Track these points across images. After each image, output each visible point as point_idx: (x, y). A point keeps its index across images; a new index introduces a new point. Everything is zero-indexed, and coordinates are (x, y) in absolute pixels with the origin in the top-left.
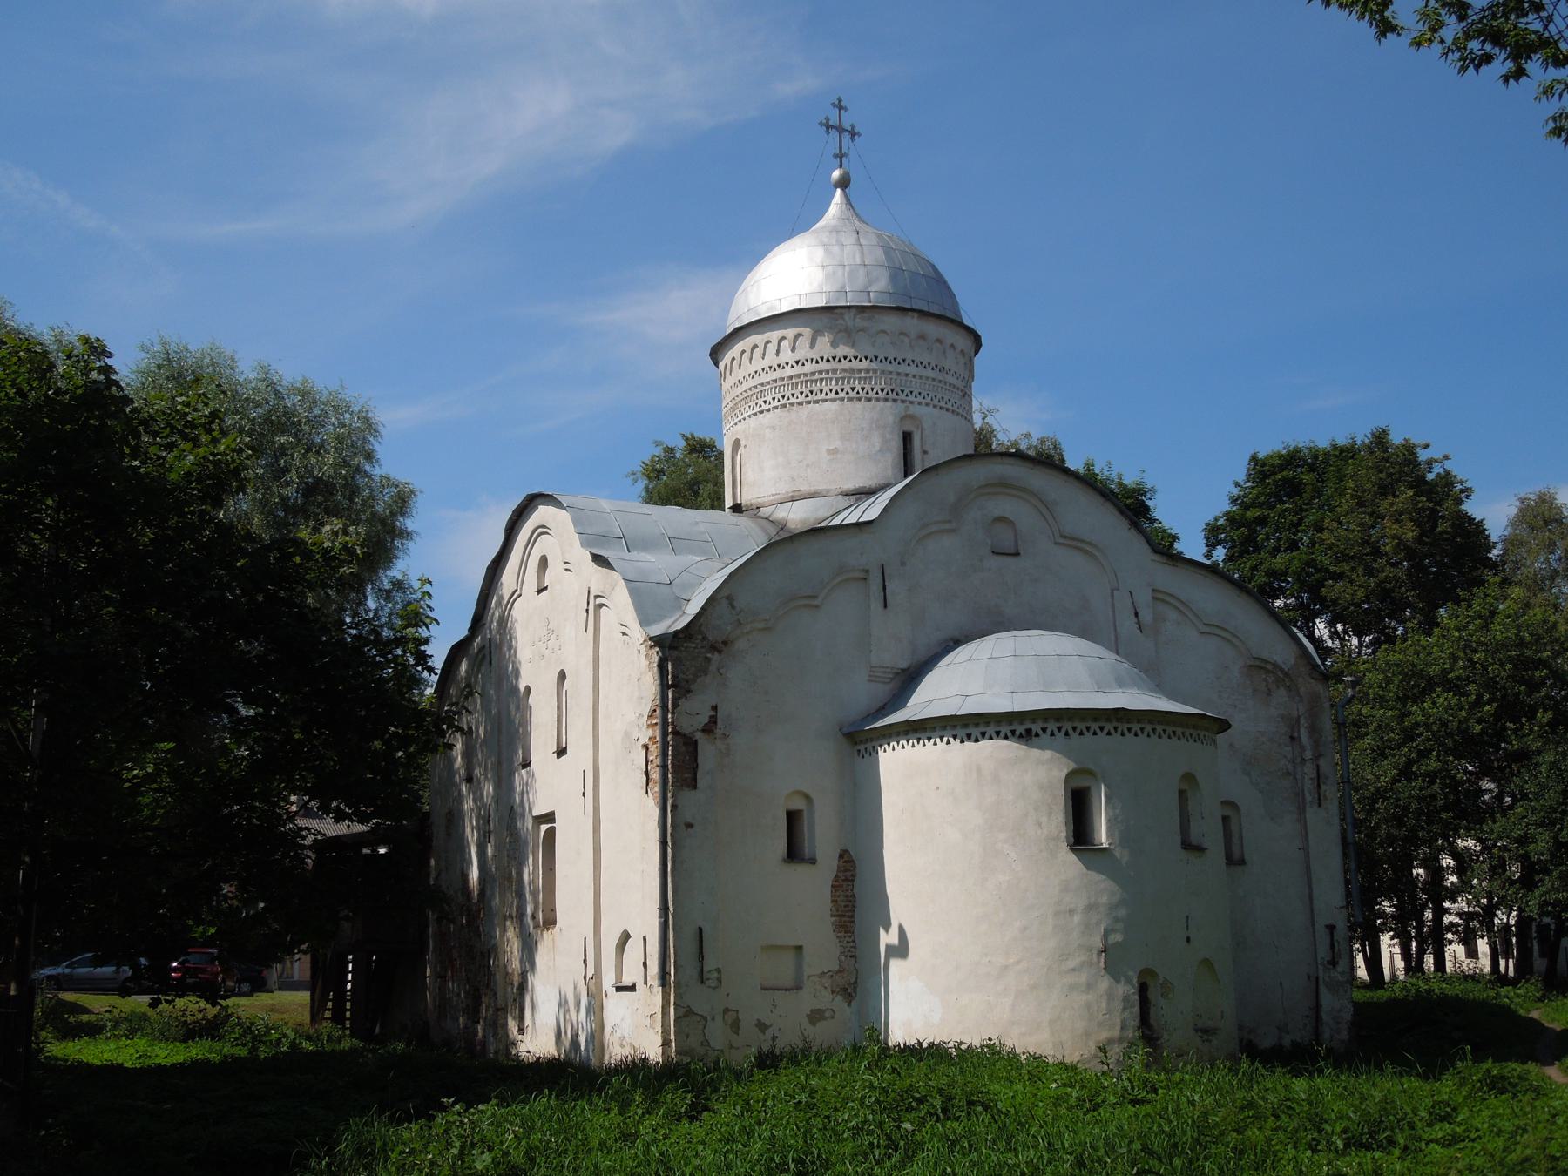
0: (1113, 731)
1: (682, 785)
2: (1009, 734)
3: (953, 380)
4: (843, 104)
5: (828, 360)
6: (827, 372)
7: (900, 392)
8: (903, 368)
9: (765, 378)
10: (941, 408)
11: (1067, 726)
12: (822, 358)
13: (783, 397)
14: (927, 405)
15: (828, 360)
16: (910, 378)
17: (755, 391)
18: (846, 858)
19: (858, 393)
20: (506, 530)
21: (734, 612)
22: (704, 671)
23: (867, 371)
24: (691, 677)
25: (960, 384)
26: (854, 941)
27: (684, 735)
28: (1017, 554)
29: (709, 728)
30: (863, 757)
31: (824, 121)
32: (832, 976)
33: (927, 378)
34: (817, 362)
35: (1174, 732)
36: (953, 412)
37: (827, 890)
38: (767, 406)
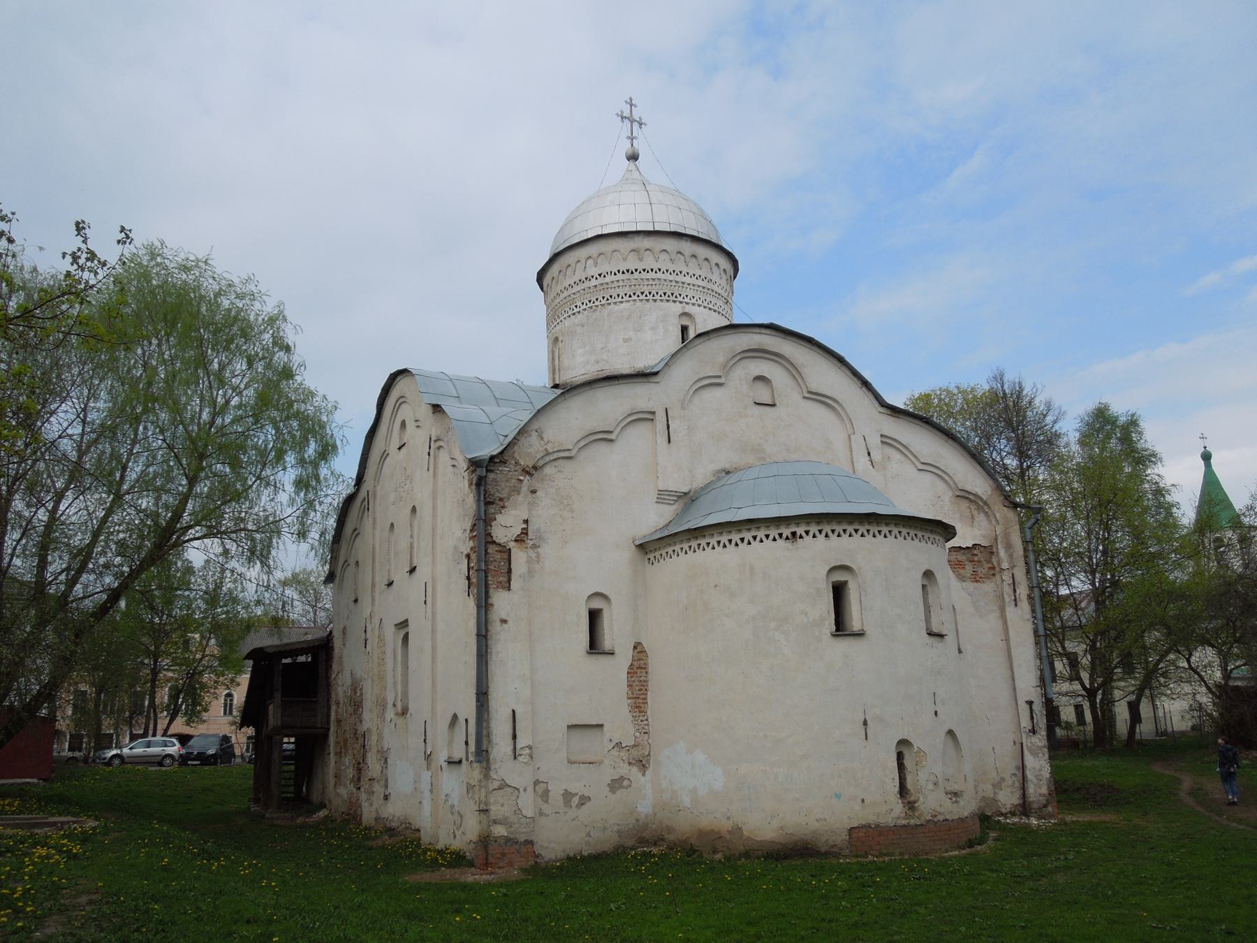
1: (498, 587)
2: (777, 537)
3: (719, 290)
4: (633, 102)
5: (623, 273)
6: (623, 280)
8: (680, 278)
9: (576, 288)
10: (710, 309)
12: (619, 271)
13: (590, 301)
14: (699, 306)
15: (623, 273)
16: (686, 285)
17: (568, 299)
18: (638, 650)
20: (377, 406)
21: (542, 442)
23: (654, 279)
25: (725, 296)
26: (647, 720)
28: (773, 405)
29: (520, 540)
30: (653, 564)
31: (620, 113)
33: (699, 286)
34: (615, 274)
36: (719, 313)
37: (624, 676)
38: (578, 310)
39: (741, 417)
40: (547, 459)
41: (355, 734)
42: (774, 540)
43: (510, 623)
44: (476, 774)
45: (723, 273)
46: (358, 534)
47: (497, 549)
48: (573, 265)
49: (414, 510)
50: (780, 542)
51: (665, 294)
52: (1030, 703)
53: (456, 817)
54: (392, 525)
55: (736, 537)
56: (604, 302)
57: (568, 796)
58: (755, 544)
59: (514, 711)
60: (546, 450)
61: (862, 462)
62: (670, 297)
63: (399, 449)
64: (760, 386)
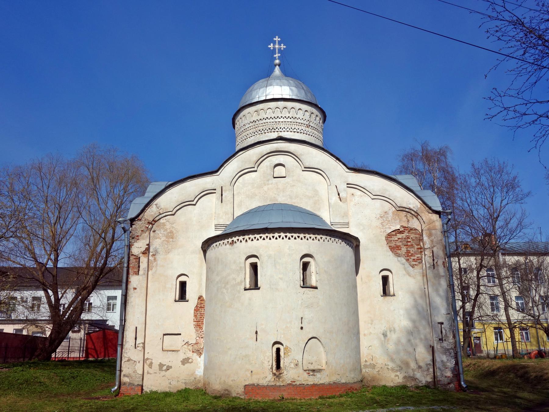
1: (133, 274)
3: (302, 121)
7: (276, 129)
8: (278, 120)
10: (294, 132)
11: (246, 237)
19: (261, 132)
29: (146, 252)
32: (193, 345)
33: (288, 122)
35: (299, 237)
37: (192, 312)
39: (265, 185)
40: (161, 216)
43: (138, 289)
47: (134, 257)
57: (161, 366)
59: (136, 327)
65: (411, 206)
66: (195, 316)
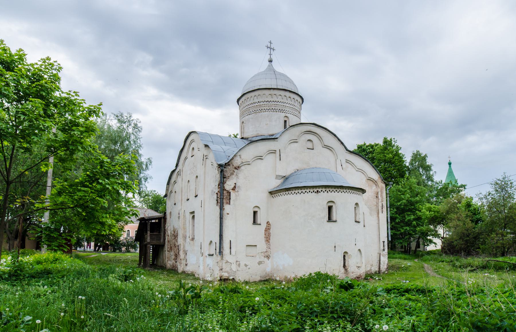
0: (339, 192)
2: (313, 192)
3: (297, 109)
8: (285, 104)
9: (250, 106)
11: (328, 190)
14: (291, 114)
16: (287, 107)
22: (232, 174)
23: (276, 105)
24: (229, 175)
25: (299, 110)
27: (227, 191)
28: (313, 149)
29: (234, 189)
37: (264, 231)
38: (251, 113)
40: (242, 164)
41: (175, 245)
42: (312, 192)
44: (219, 258)
45: (299, 103)
46: (176, 183)
48: (250, 98)
49: (197, 177)
50: (313, 193)
51: (280, 110)
52: (384, 242)
53: (211, 271)
54: (189, 181)
55: (300, 191)
56: (259, 111)
57: (246, 265)
58: (306, 194)
59: (230, 241)
60: (242, 161)
61: (339, 167)
62: (281, 111)
63: (192, 157)
64: (309, 142)
65: (374, 178)
66: (265, 234)
